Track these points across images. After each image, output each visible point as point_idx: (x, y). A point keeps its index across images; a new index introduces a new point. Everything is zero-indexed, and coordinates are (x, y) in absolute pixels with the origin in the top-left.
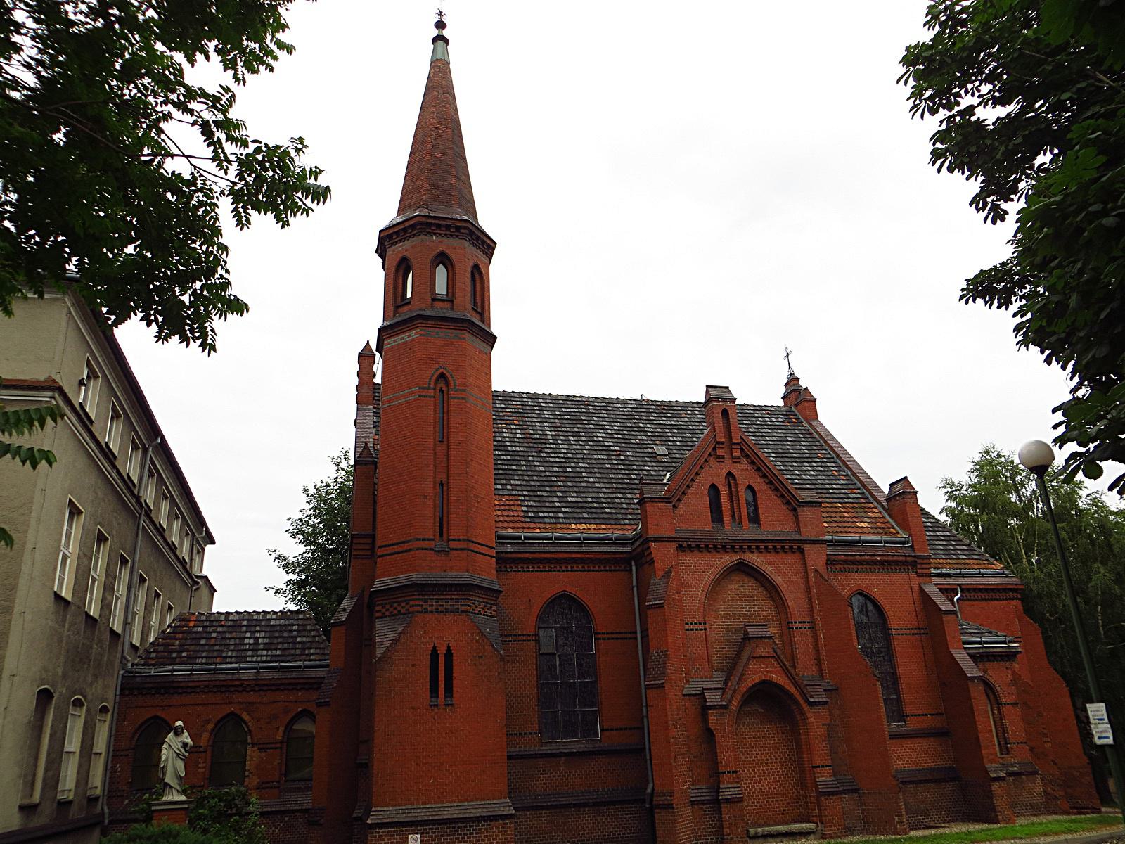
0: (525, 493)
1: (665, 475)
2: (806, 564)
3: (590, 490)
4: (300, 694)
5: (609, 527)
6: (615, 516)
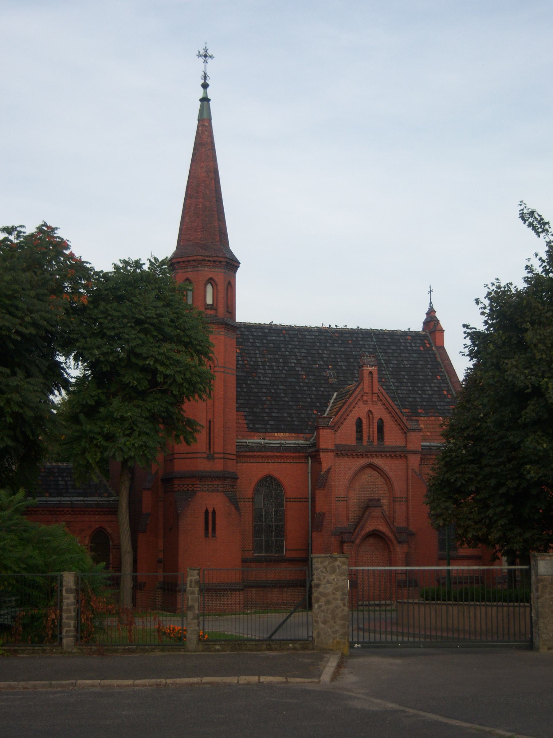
1: (333, 395)
2: (407, 465)
4: (97, 517)
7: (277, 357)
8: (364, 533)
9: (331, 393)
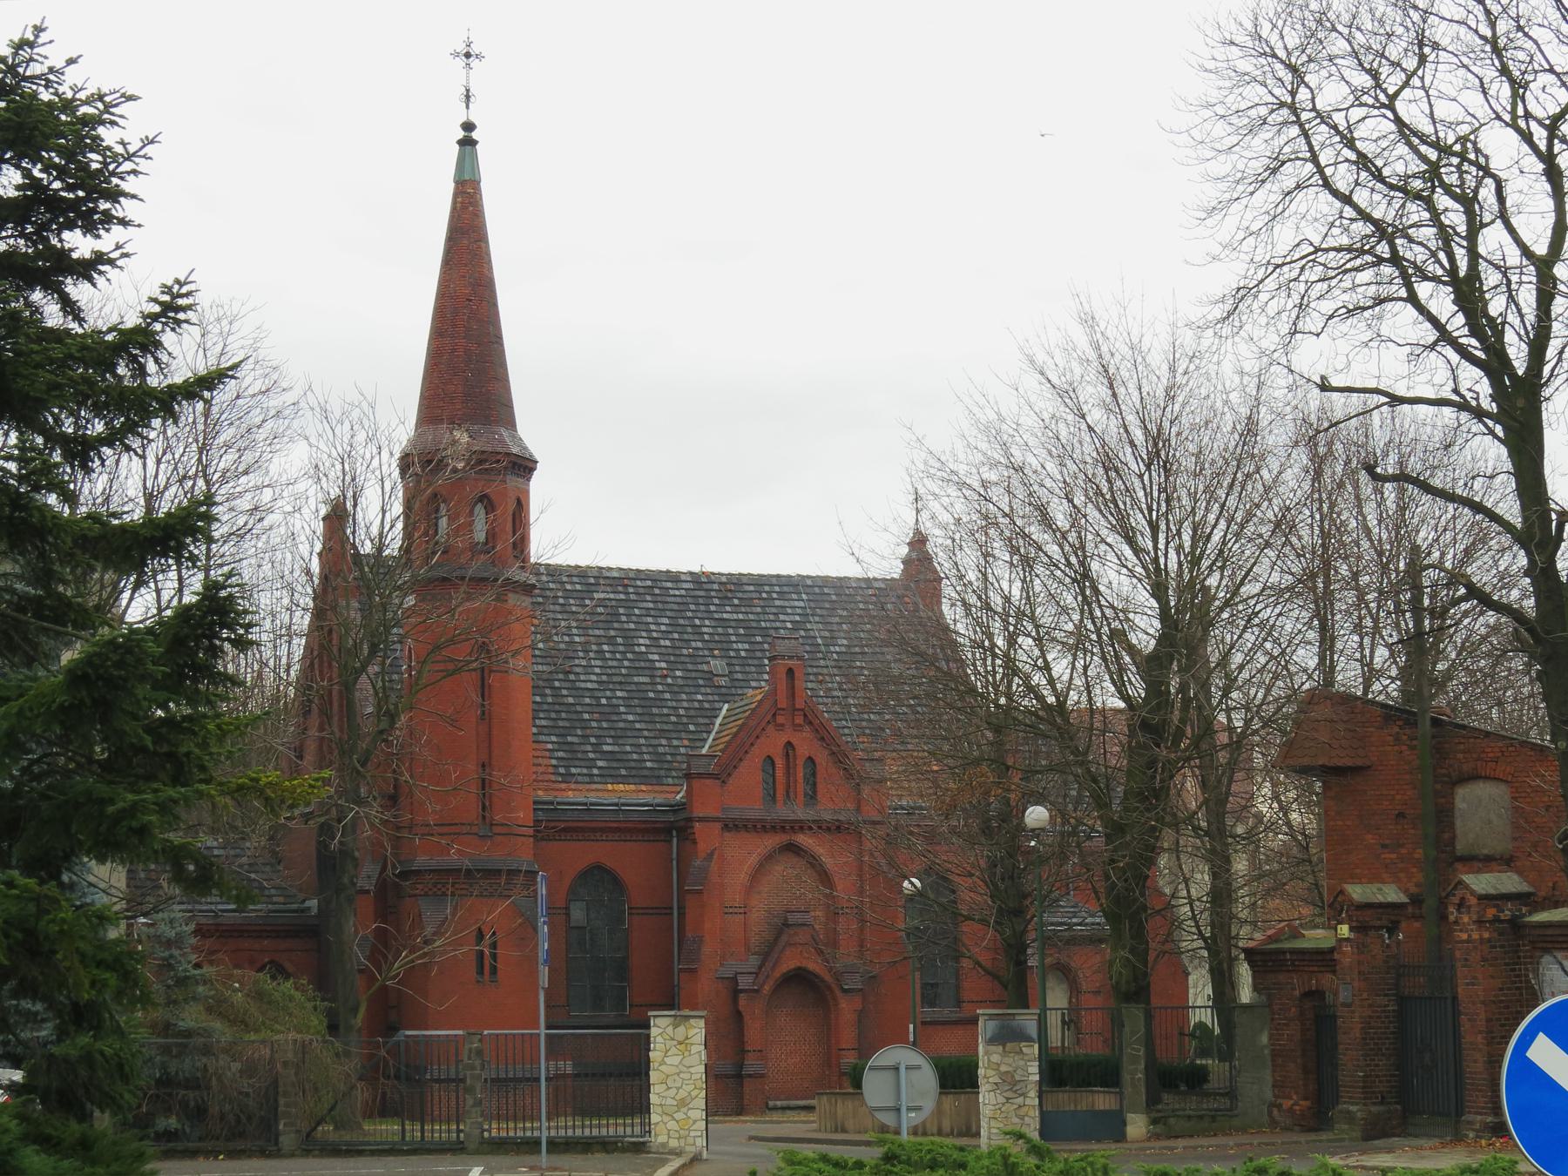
0: (554, 739)
1: (721, 709)
3: (629, 734)
5: (650, 788)
6: (656, 773)
7: (612, 633)
8: (777, 974)
9: (717, 705)
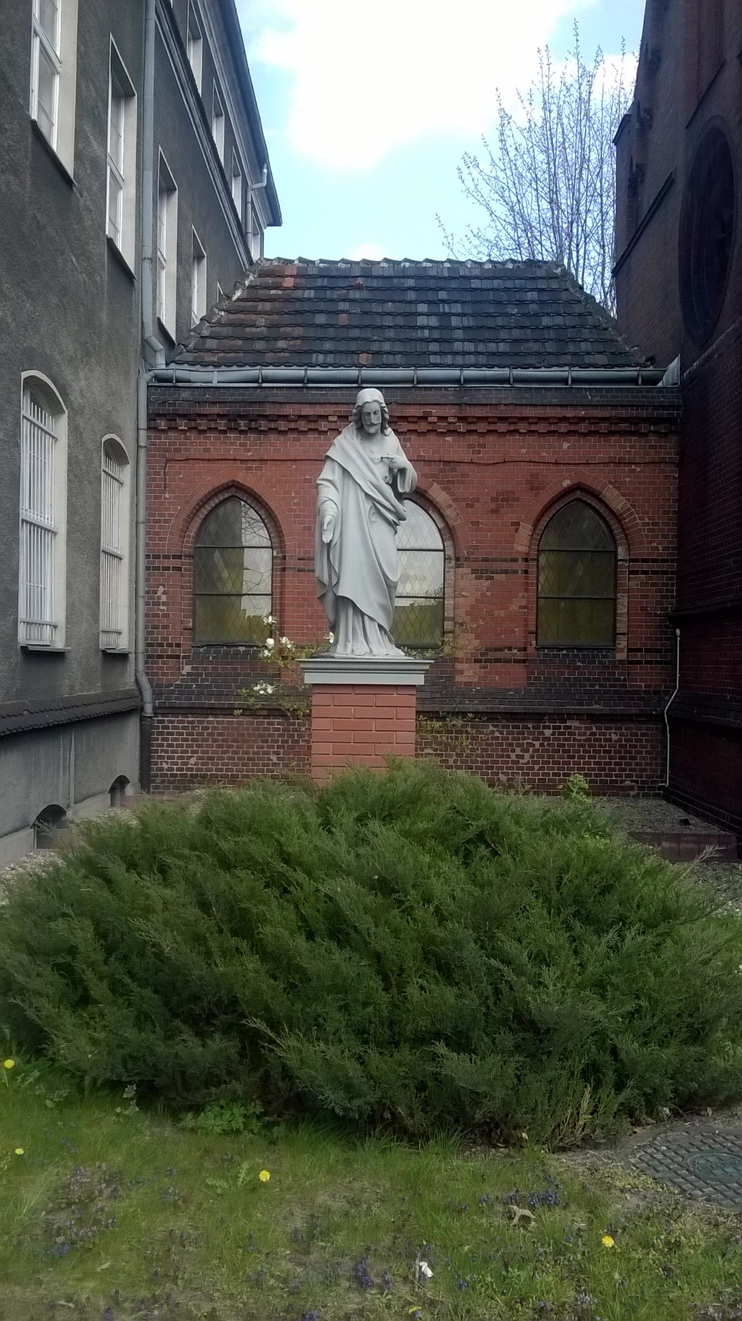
4: (565, 445)
